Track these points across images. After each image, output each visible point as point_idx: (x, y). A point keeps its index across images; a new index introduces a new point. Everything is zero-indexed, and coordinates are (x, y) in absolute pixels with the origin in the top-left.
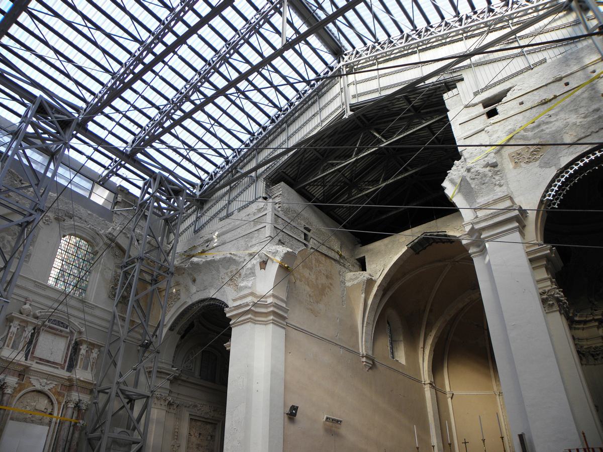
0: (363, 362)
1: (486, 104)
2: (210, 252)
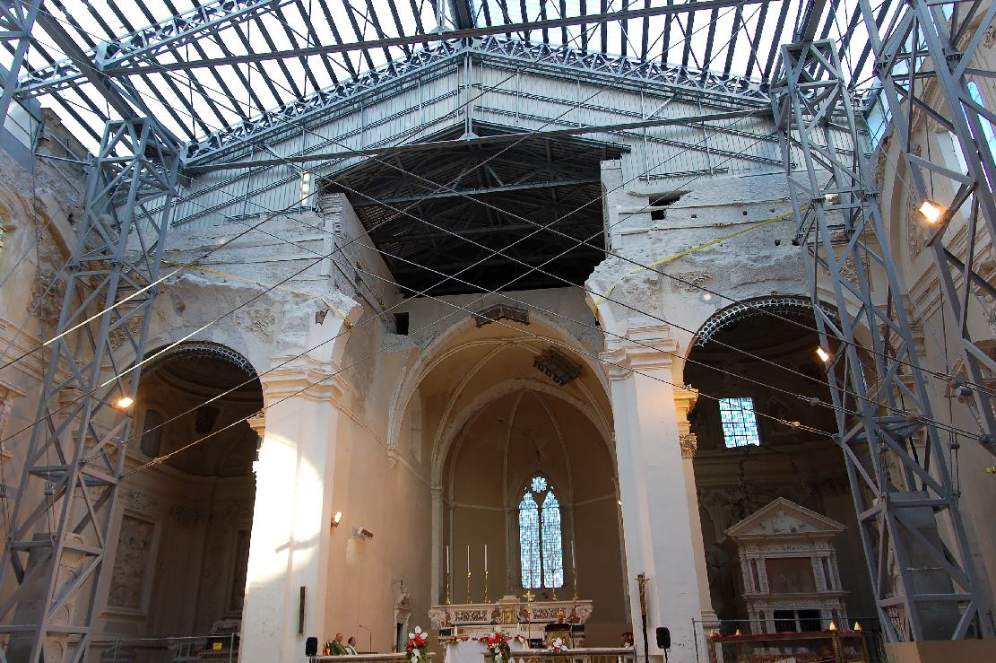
1: (654, 200)
2: (211, 269)
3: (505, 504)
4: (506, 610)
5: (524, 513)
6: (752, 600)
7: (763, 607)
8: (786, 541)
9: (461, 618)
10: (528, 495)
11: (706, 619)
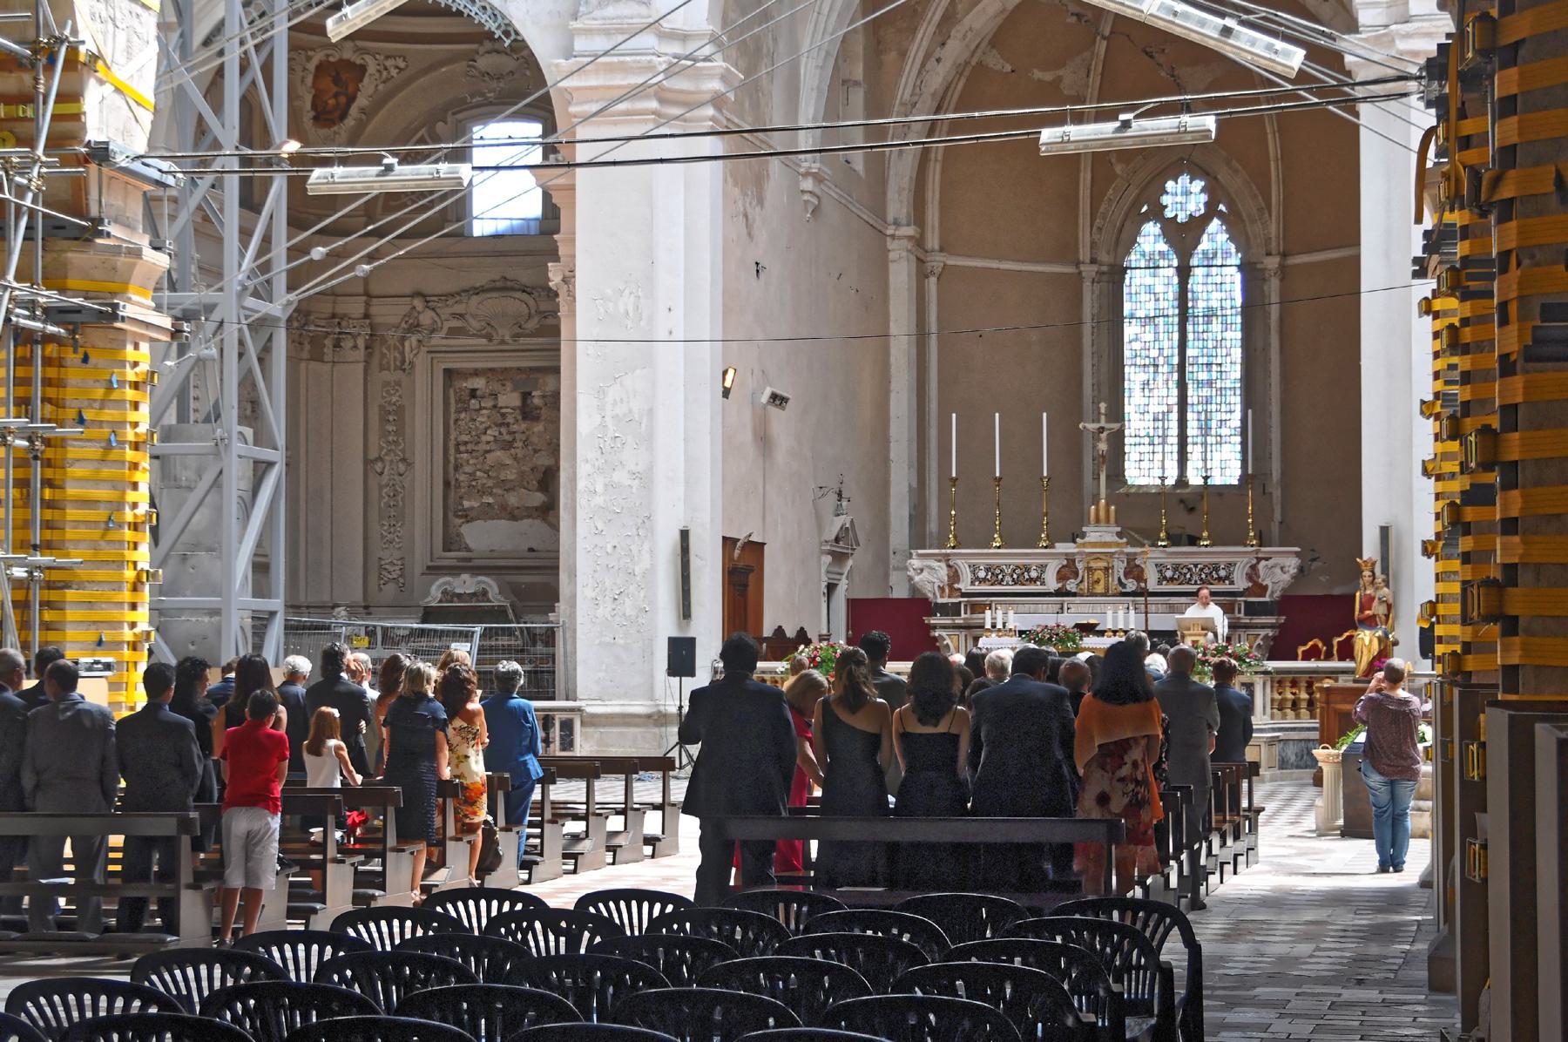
3: (1084, 253)
4: (1093, 564)
5: (1136, 280)
9: (984, 580)
10: (1151, 229)
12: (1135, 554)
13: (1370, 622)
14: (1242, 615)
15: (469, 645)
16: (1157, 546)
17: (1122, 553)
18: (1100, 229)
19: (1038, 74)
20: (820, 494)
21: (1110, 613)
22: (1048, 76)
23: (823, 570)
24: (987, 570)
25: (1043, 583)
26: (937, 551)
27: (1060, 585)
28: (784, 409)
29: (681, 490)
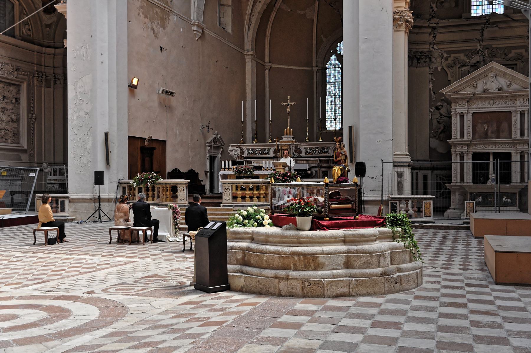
0: (193, 30)
3: (314, 64)
4: (283, 148)
6: (456, 145)
7: (465, 149)
8: (493, 99)
10: (334, 57)
11: (397, 160)
12: (298, 144)
13: (338, 163)
14: (332, 164)
15: (35, 174)
16: (305, 142)
17: (293, 144)
18: (319, 57)
19: (299, 12)
20: (203, 127)
21: (264, 162)
22: (302, 13)
23: (207, 151)
24: (252, 150)
25: (269, 155)
26: (237, 145)
27: (274, 155)
28: (174, 96)
29: (107, 119)
